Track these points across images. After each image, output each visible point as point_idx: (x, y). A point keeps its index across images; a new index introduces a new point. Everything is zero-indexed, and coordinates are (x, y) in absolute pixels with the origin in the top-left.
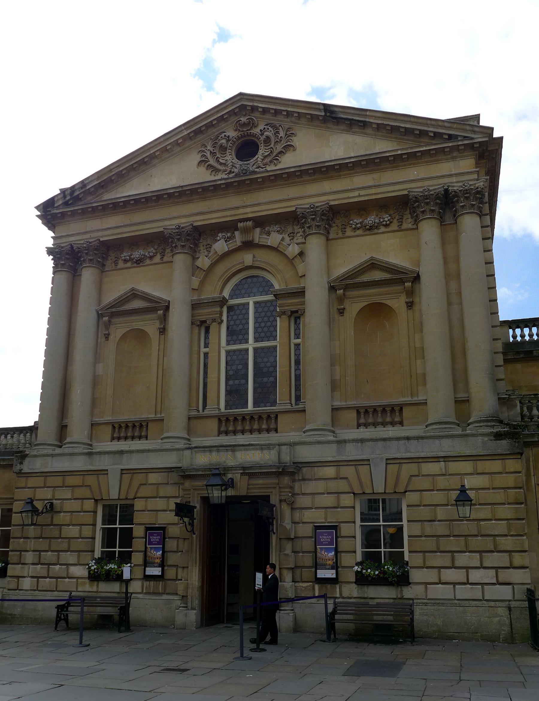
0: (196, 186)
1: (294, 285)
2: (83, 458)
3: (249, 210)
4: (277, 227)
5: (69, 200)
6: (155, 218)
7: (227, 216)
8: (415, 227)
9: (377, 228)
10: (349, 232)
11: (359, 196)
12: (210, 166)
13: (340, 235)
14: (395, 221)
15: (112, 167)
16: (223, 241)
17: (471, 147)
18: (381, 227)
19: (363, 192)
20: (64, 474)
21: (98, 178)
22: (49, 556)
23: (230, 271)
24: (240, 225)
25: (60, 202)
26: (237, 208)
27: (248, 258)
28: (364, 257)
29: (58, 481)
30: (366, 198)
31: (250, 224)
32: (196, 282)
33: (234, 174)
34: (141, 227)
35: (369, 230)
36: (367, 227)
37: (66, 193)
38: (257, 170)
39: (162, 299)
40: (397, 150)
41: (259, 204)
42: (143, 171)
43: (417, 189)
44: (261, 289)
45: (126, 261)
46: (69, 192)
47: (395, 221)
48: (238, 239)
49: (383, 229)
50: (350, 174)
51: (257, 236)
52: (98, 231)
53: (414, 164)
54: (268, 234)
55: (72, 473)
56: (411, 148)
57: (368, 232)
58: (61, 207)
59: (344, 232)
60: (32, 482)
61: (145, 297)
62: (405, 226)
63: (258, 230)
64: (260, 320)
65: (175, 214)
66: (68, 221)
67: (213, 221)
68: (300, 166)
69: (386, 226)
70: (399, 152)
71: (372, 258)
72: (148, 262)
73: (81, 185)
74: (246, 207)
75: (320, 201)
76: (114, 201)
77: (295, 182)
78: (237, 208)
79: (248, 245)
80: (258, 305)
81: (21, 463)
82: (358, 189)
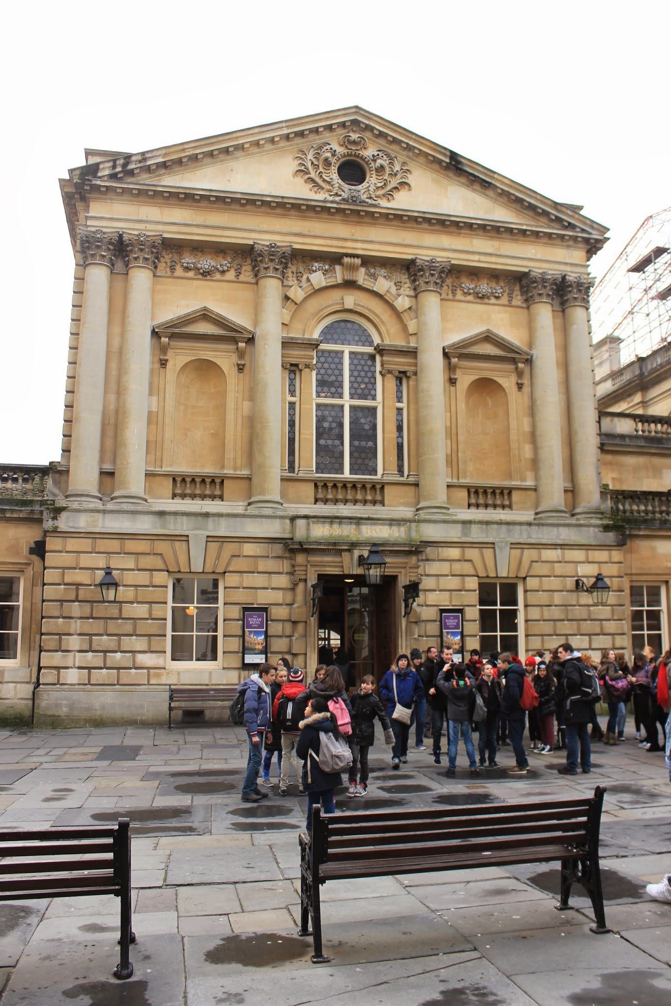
0: (301, 202)
1: (399, 342)
3: (359, 245)
4: (383, 272)
5: (120, 172)
6: (239, 226)
7: (331, 246)
8: (524, 305)
9: (488, 298)
10: (459, 296)
11: (479, 261)
12: (312, 180)
13: (450, 296)
14: (505, 294)
15: (186, 146)
16: (319, 274)
17: (587, 241)
18: (492, 298)
19: (483, 258)
20: (122, 536)
21: (165, 155)
23: (325, 311)
24: (346, 260)
25: (107, 172)
26: (345, 240)
28: (477, 329)
29: (114, 545)
30: (486, 265)
31: (358, 261)
32: (286, 317)
33: (340, 198)
34: (219, 232)
35: (480, 298)
36: (480, 295)
37: (118, 162)
38: (368, 200)
39: (245, 329)
40: (522, 224)
41: (371, 242)
42: (222, 161)
43: (537, 269)
44: (357, 338)
46: (121, 162)
47: (505, 294)
48: (339, 274)
49: (493, 301)
50: (471, 234)
51: (361, 276)
52: (158, 223)
53: (533, 242)
54: (374, 277)
55: (134, 536)
56: (536, 226)
57: (478, 300)
58: (106, 179)
59: (454, 294)
60: (73, 544)
61: (220, 322)
62: (514, 302)
63: (363, 270)
64: (356, 373)
65: (265, 227)
66: (111, 199)
67: (315, 248)
68: (424, 213)
69: (497, 298)
70: (525, 227)
71: (488, 331)
72: (218, 276)
73: (140, 158)
74: (356, 241)
75: (442, 257)
76: (188, 191)
77: (412, 228)
78: (345, 240)
79: (350, 285)
80: (353, 356)
82: (480, 253)
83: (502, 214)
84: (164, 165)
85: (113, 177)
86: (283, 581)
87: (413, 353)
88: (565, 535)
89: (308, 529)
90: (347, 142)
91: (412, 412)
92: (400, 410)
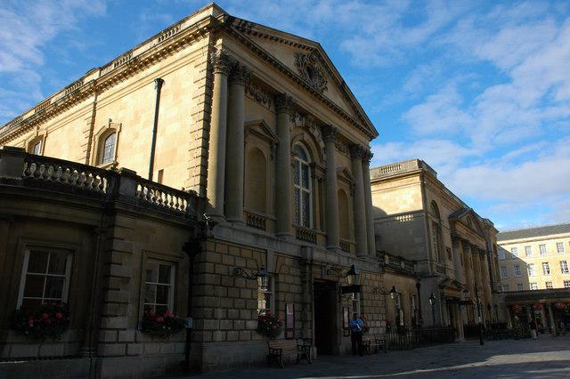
2: (252, 237)
22: (233, 312)
24: (310, 117)
27: (306, 137)
45: (252, 94)
79: (306, 128)
81: (211, 229)
83: (350, 113)
84: (255, 34)
85: (237, 28)
86: (298, 280)
87: (324, 171)
88: (371, 268)
89: (312, 253)
90: (311, 59)
91: (317, 198)
92: (308, 194)
